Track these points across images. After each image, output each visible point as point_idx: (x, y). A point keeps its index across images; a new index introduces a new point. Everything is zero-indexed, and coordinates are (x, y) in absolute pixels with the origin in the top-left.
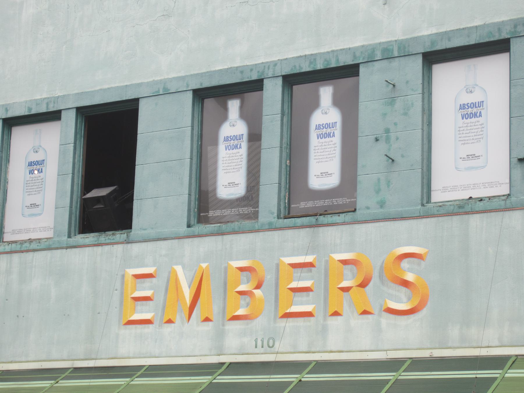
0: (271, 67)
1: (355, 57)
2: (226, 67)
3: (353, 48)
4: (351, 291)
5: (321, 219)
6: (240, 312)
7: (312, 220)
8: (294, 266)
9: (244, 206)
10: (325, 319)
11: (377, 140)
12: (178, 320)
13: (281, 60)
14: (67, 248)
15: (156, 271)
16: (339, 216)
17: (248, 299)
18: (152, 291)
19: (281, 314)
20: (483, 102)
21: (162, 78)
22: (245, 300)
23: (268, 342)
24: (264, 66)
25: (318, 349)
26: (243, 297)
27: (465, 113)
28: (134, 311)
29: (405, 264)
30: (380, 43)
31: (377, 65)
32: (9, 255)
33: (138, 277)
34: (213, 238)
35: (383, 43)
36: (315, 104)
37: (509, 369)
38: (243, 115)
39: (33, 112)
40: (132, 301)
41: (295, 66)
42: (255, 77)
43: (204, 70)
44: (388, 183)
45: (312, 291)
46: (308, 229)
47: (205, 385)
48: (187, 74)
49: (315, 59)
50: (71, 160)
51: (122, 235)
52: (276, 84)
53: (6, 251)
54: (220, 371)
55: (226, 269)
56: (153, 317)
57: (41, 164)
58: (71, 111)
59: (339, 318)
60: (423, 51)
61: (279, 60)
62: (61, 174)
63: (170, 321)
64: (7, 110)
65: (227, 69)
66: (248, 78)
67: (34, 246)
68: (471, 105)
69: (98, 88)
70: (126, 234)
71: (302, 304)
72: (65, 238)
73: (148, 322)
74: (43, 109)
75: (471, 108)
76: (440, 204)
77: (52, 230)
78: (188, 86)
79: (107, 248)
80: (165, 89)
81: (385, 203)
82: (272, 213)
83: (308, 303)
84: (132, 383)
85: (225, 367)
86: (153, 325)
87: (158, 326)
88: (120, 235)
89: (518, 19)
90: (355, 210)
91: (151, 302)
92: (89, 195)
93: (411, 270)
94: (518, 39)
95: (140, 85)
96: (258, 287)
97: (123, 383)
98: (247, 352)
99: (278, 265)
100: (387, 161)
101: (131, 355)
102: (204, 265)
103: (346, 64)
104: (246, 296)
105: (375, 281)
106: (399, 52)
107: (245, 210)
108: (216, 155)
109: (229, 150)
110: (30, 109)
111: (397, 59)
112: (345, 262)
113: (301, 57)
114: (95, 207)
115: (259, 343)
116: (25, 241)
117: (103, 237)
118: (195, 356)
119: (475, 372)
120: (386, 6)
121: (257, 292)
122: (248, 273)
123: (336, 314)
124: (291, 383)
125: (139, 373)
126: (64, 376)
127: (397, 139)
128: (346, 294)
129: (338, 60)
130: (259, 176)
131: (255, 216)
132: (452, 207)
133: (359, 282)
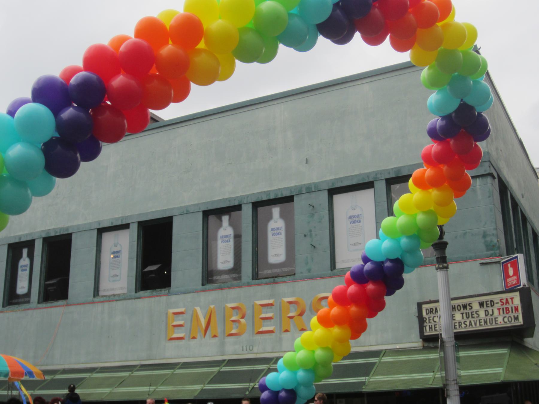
1: (291, 191)
2: (221, 198)
3: (290, 187)
4: (294, 319)
5: (276, 279)
6: (233, 331)
7: (272, 280)
8: (262, 305)
9: (233, 273)
12: (198, 337)
13: (251, 194)
14: (135, 299)
15: (185, 310)
16: (286, 277)
17: (237, 324)
19: (256, 331)
20: (361, 214)
21: (185, 205)
23: (250, 348)
27: (352, 220)
28: (174, 333)
30: (305, 184)
31: (303, 196)
33: (175, 314)
35: (307, 184)
36: (270, 217)
37: (383, 357)
38: (231, 224)
39: (114, 224)
41: (259, 197)
42: (237, 203)
43: (208, 200)
44: (312, 259)
46: (269, 285)
47: (216, 372)
48: (200, 202)
49: (269, 194)
50: (136, 250)
51: (166, 291)
54: (223, 364)
55: (224, 309)
57: (119, 253)
58: (135, 223)
59: (288, 333)
60: (328, 188)
61: (250, 194)
62: (130, 258)
63: (194, 338)
64: (99, 224)
65: (222, 199)
66: (233, 204)
67: (116, 298)
68: (355, 216)
69: (150, 211)
70: (167, 291)
71: (267, 326)
72: (133, 293)
74: (119, 223)
75: (355, 218)
76: (341, 270)
77: (126, 289)
78: (200, 209)
79: (157, 298)
80: (187, 211)
83: (271, 326)
84: (175, 372)
85: (226, 362)
88: (164, 291)
89: (378, 171)
90: (295, 274)
91: (183, 328)
92: (146, 270)
94: (378, 181)
95: (173, 209)
96: (243, 317)
97: (170, 373)
99: (253, 306)
100: (311, 247)
102: (212, 306)
104: (236, 323)
105: (307, 312)
107: (234, 276)
108: (216, 247)
109: (223, 243)
110: (112, 223)
111: (314, 193)
112: (290, 303)
113: (261, 192)
114: (150, 276)
115: (245, 348)
116: (111, 295)
117: (155, 293)
118: (209, 356)
119: (366, 359)
121: (243, 321)
123: (287, 331)
124: (264, 369)
125: (178, 367)
126: (135, 369)
127: (316, 235)
128: (292, 320)
129: (282, 194)
130: (241, 256)
131: (240, 278)
133: (298, 313)
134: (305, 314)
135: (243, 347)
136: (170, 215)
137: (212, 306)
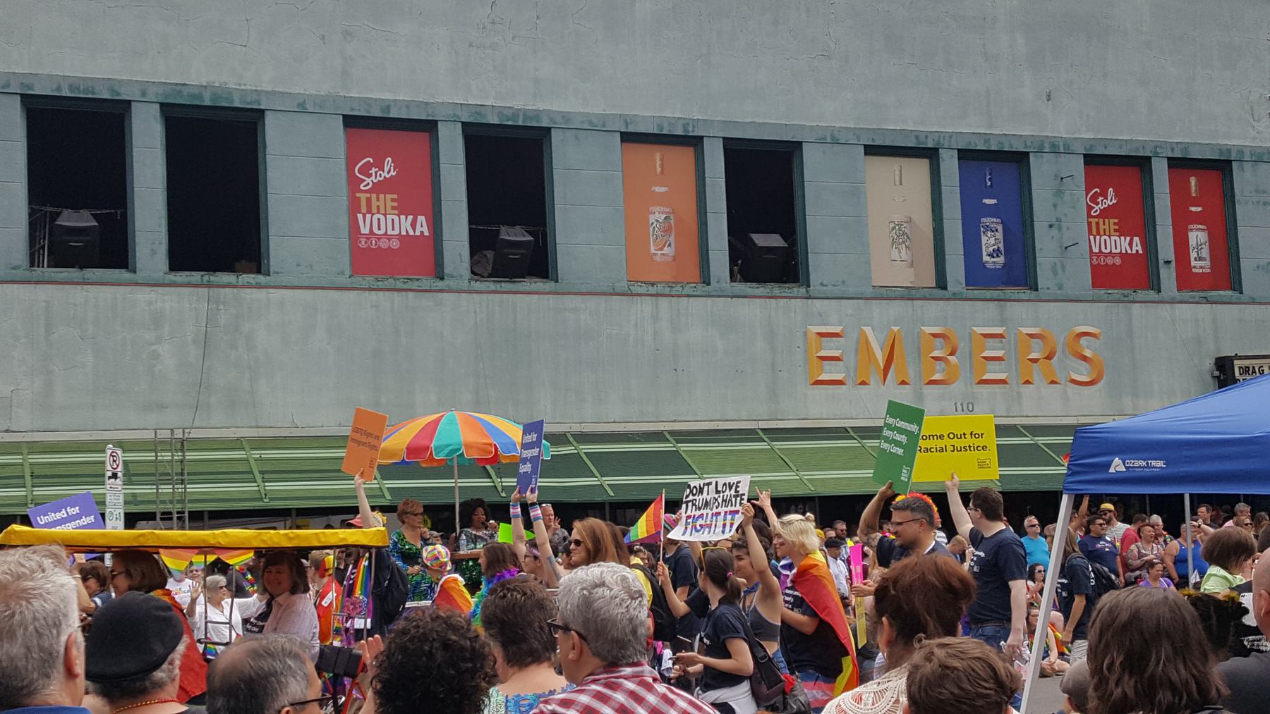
0: (947, 138)
6: (937, 377)
8: (986, 336)
11: (1051, 226)
12: (872, 381)
14: (732, 297)
17: (942, 364)
18: (840, 351)
22: (940, 365)
23: (968, 407)
24: (940, 136)
25: (1015, 414)
26: (938, 362)
28: (821, 371)
29: (1084, 341)
32: (654, 298)
33: (821, 335)
34: (902, 302)
40: (819, 360)
45: (1004, 360)
51: (800, 290)
52: (953, 157)
53: (649, 293)
56: (844, 377)
63: (863, 383)
80: (833, 137)
81: (1062, 285)
86: (846, 386)
93: (1088, 348)
96: (952, 354)
99: (972, 334)
101: (824, 417)
102: (896, 329)
103: (1018, 150)
106: (1064, 148)
111: (1062, 155)
112: (1032, 336)
115: (959, 407)
120: (1050, 102)
127: (1068, 228)
132: (1118, 296)
134: (1056, 358)
136: (800, 140)
137: (896, 329)
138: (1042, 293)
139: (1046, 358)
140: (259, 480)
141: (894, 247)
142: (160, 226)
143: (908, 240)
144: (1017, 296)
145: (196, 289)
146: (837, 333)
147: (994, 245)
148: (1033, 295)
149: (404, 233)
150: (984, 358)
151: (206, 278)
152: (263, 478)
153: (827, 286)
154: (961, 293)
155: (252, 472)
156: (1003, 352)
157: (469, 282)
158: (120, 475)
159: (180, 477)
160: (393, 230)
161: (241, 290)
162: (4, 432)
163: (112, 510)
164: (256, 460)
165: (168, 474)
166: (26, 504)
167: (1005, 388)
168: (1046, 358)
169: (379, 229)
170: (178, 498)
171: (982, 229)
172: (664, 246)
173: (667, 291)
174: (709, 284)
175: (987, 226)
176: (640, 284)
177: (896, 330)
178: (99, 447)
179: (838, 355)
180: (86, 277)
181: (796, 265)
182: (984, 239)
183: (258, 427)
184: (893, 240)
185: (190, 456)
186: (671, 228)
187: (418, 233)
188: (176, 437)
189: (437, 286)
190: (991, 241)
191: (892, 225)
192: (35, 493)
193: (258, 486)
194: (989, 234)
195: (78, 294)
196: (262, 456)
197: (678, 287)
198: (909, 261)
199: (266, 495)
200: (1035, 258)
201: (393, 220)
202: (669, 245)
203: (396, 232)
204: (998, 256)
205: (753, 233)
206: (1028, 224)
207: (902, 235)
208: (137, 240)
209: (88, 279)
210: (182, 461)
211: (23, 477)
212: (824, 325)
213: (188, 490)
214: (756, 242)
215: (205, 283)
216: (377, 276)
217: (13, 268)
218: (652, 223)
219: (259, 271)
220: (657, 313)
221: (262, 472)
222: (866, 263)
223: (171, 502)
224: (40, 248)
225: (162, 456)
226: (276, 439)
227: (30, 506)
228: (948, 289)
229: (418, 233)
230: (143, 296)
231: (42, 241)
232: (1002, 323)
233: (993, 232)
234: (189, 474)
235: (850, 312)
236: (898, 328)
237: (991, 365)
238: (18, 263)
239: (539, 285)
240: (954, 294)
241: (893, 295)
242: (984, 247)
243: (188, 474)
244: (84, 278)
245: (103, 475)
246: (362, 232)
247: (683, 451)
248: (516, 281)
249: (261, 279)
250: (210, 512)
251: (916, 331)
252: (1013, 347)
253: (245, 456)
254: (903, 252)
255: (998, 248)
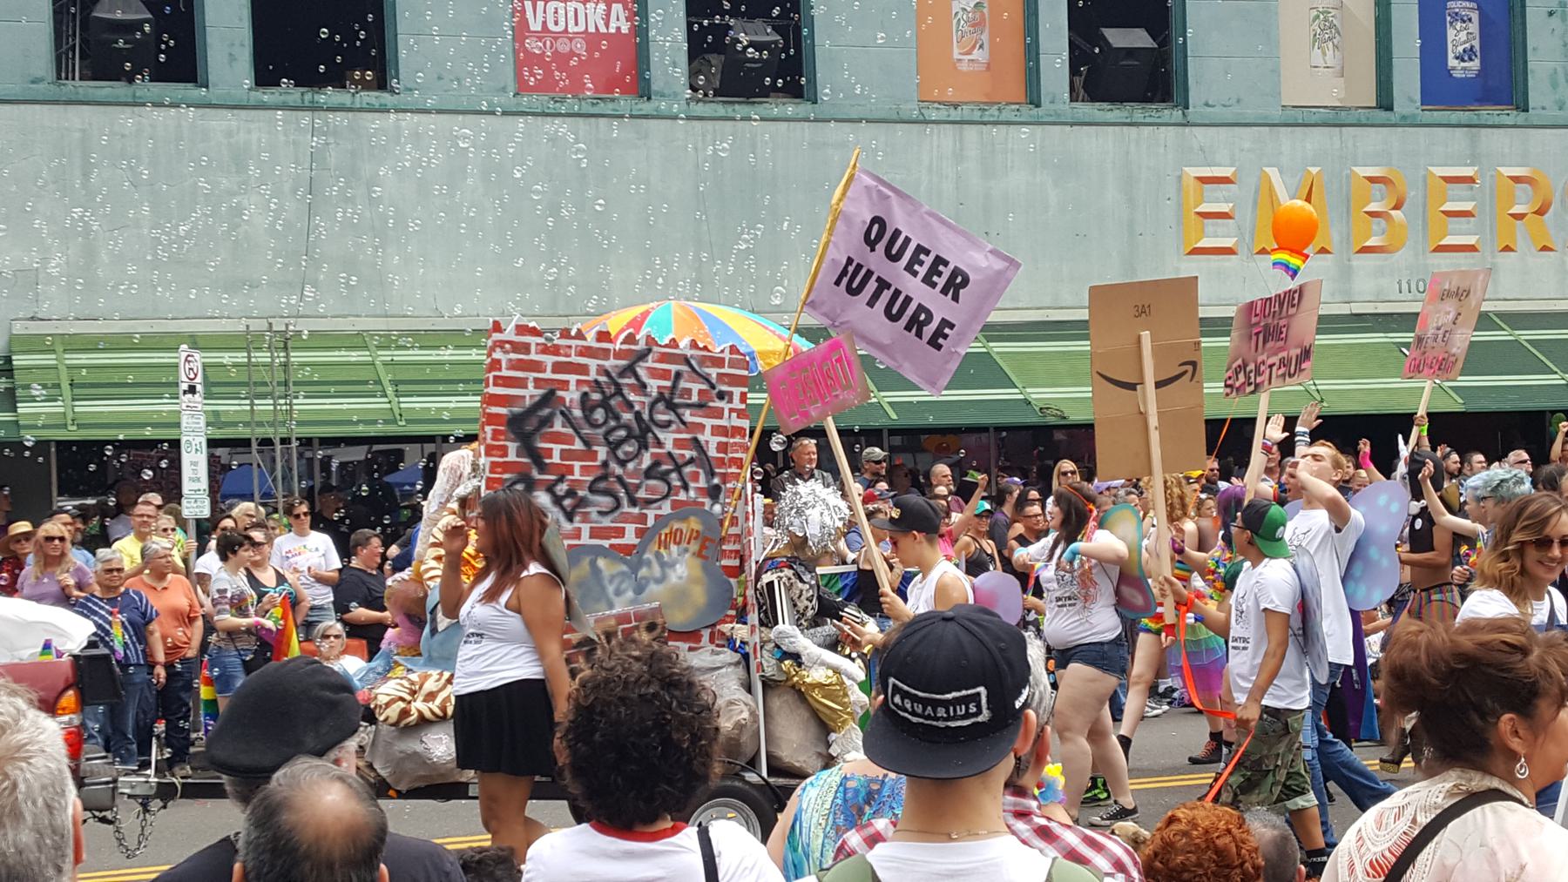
8: (1449, 180)
10: (1493, 257)
14: (1072, 124)
15: (1234, 174)
18: (1231, 205)
23: (1417, 286)
28: (1202, 234)
45: (1473, 216)
51: (1175, 113)
53: (950, 119)
73: (1229, 251)
81: (1564, 104)
82: (1412, 100)
87: (1245, 258)
88: (1172, 114)
96: (1396, 207)
98: (1387, 299)
112: (1516, 179)
115: (1405, 287)
121: (1397, 215)
122: (1382, 186)
123: (1507, 249)
128: (1518, 222)
135: (1400, 283)
137: (1314, 170)
138: (1534, 115)
139: (1534, 213)
140: (390, 390)
141: (1316, 47)
142: (241, 20)
143: (1338, 37)
144: (1497, 120)
145: (294, 113)
146: (1227, 178)
147: (1465, 42)
148: (1521, 118)
149: (592, 29)
150: (1443, 212)
151: (308, 97)
152: (397, 391)
153: (1213, 106)
154: (1414, 116)
155: (378, 382)
156: (1474, 203)
157: (688, 104)
158: (199, 388)
159: (283, 388)
160: (576, 24)
161: (358, 114)
162: (28, 319)
163: (188, 438)
164: (385, 364)
165: (265, 384)
166: (65, 426)
167: (1473, 257)
168: (1534, 213)
169: (556, 23)
170: (280, 418)
171: (1448, 18)
172: (974, 47)
173: (977, 116)
174: (1038, 106)
175: (1457, 14)
176: (936, 105)
177: (1314, 173)
178: (167, 343)
179: (1227, 210)
180: (137, 94)
181: (1168, 73)
182: (1451, 33)
183: (387, 317)
184: (1315, 35)
185: (297, 357)
186: (984, 20)
187: (612, 31)
188: (275, 329)
189: (641, 110)
190: (1461, 37)
191: (1315, 13)
192: (76, 409)
193: (390, 402)
194: (1459, 25)
195: (126, 119)
196: (395, 358)
197: (994, 110)
198: (1338, 68)
199: (401, 415)
200: (1526, 62)
201: (576, 10)
202: (981, 47)
203: (581, 28)
204: (1471, 59)
205: (1107, 27)
206: (1518, 9)
207: (1328, 29)
208: (209, 40)
209: (140, 98)
210: (285, 365)
211: (58, 386)
212: (1209, 166)
213: (295, 407)
214: (1111, 41)
215: (307, 104)
216: (553, 95)
217: (33, 82)
218: (957, 13)
219: (381, 84)
220: (961, 150)
221: (395, 383)
222: (1272, 71)
223: (272, 424)
224: (67, 50)
225: (255, 357)
226: (414, 333)
227: (70, 428)
228: (1395, 109)
229: (612, 31)
230: (221, 122)
231: (70, 39)
232: (1474, 160)
233: (1464, 22)
234: (295, 384)
235: (1247, 145)
236: (1319, 168)
237: (1454, 223)
238: (40, 73)
239: (791, 108)
240: (1404, 117)
241: (1313, 119)
242: (1450, 46)
243: (295, 384)
244: (134, 96)
245: (177, 385)
246: (532, 29)
247: (998, 353)
248: (754, 102)
249: (385, 98)
250: (320, 439)
251: (1344, 173)
252: (1488, 196)
253: (370, 359)
254: (1330, 53)
255: (1472, 47)
